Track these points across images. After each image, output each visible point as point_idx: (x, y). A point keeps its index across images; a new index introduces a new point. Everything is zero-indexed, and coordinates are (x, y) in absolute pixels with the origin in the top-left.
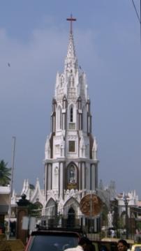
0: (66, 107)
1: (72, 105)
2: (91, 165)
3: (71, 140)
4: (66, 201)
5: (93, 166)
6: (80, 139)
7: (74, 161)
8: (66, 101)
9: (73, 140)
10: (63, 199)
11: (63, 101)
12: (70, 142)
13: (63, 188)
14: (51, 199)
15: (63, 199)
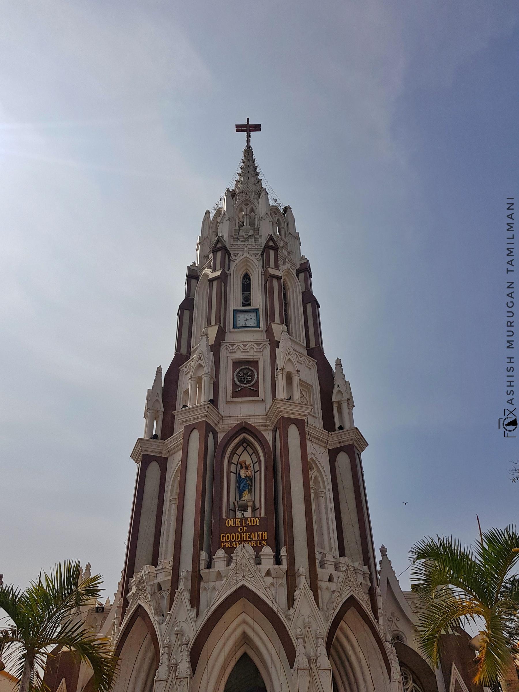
0: (226, 266)
1: (246, 260)
2: (333, 454)
3: (240, 356)
4: (207, 612)
5: (343, 459)
6: (275, 345)
7: (253, 422)
8: (225, 250)
9: (251, 355)
10: (195, 602)
11: (215, 251)
12: (236, 364)
13: (198, 547)
14: (140, 610)
15: (195, 602)
